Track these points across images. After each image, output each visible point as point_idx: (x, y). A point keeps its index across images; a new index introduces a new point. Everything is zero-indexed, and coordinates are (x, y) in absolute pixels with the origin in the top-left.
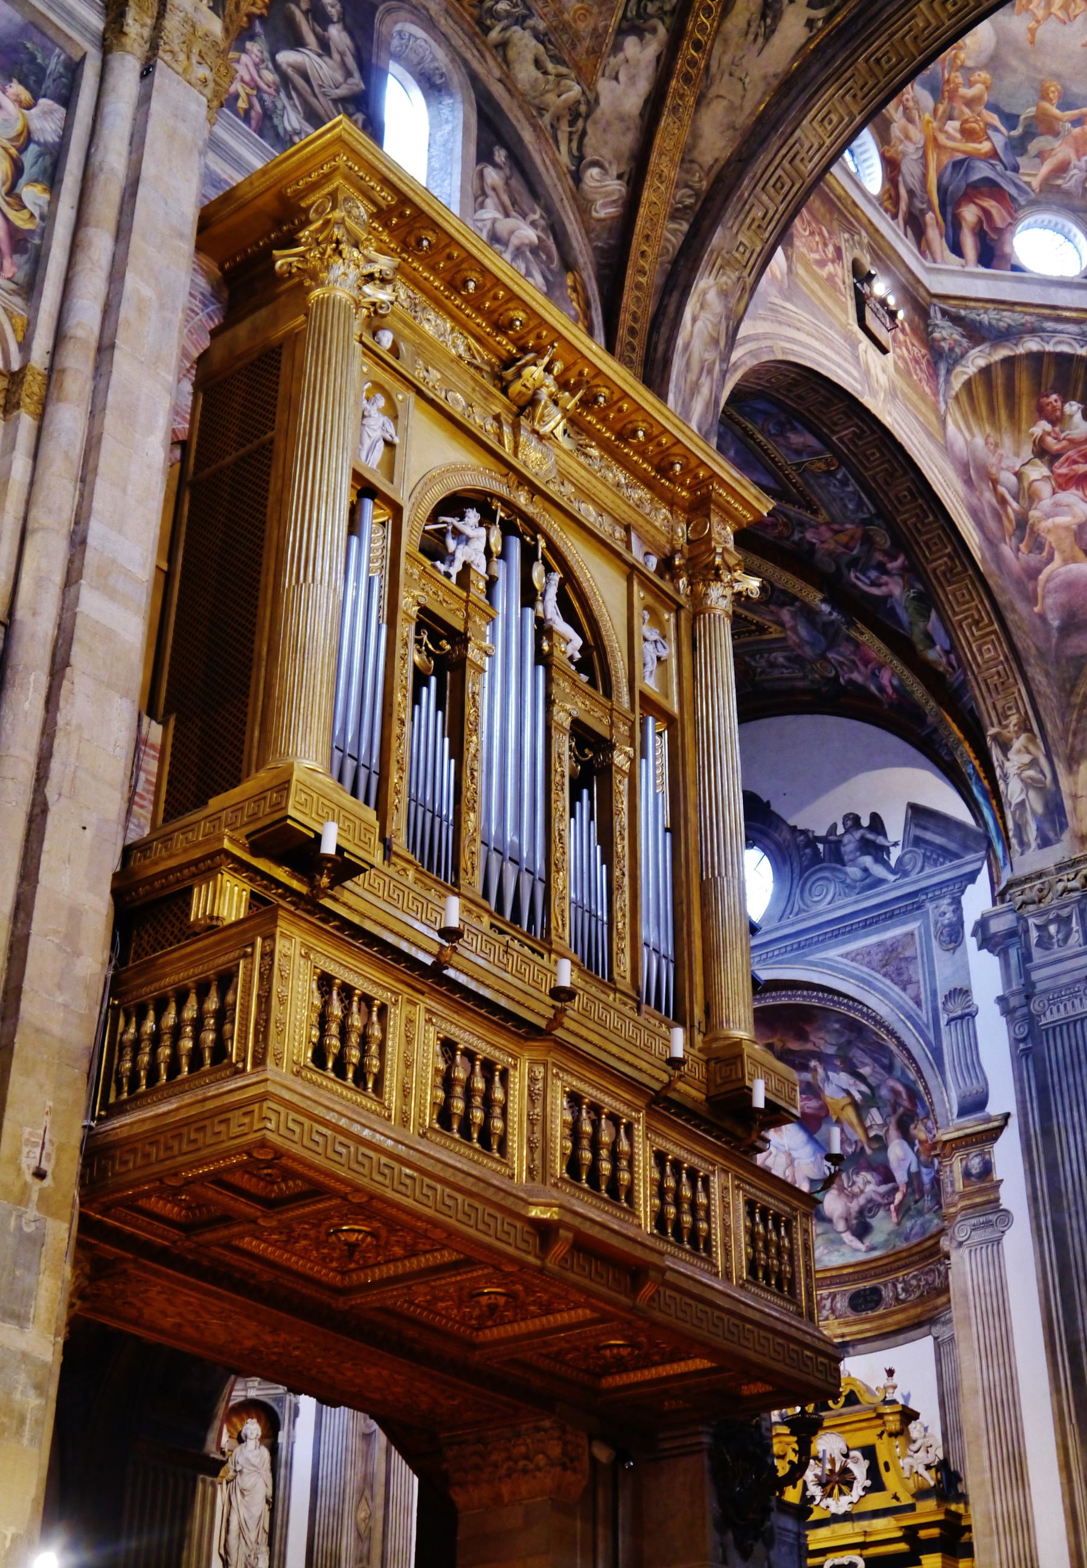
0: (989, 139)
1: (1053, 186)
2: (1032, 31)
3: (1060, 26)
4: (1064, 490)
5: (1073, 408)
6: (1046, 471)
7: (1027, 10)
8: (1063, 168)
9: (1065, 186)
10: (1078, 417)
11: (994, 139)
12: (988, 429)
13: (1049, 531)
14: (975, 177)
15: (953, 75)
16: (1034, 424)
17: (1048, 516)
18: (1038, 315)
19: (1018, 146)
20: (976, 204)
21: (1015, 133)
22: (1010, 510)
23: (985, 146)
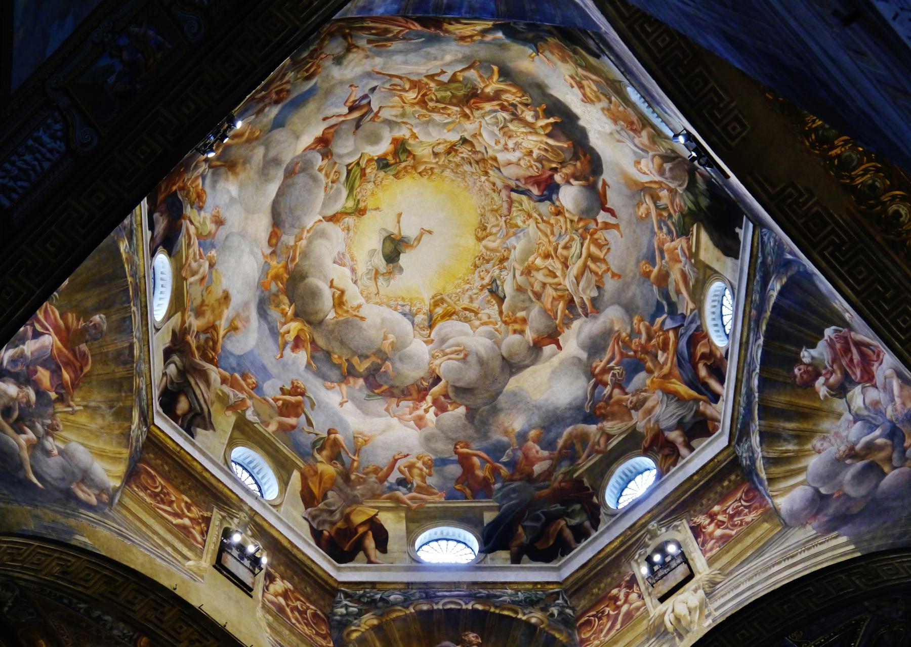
0: (668, 331)
2: (614, 275)
4: (873, 377)
5: (806, 355)
6: (858, 389)
7: (601, 277)
8: (684, 275)
10: (814, 352)
12: (809, 446)
13: (904, 404)
15: (633, 346)
16: (816, 393)
17: (892, 400)
20: (697, 363)
22: (880, 441)
23: (671, 334)
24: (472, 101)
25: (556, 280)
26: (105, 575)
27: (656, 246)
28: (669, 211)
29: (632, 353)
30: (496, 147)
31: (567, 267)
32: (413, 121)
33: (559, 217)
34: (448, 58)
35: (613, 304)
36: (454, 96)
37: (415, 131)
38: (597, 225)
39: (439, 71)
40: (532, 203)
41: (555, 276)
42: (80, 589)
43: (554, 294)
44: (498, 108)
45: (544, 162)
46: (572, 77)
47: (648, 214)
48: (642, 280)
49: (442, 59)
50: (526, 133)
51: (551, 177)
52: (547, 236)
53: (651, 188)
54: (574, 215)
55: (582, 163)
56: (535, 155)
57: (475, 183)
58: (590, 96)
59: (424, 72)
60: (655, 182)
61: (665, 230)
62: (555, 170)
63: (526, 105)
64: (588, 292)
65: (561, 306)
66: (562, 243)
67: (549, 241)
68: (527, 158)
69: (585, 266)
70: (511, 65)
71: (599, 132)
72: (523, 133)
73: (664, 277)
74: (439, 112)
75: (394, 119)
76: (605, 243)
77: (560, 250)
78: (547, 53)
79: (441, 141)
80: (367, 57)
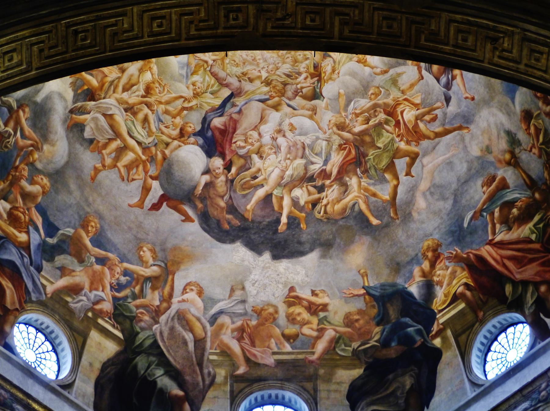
0: (28, 233)
1: (63, 299)
2: (97, 171)
3: (119, 180)
7: (100, 152)
8: (75, 290)
9: (72, 305)
11: (31, 235)
14: (6, 257)
15: (22, 166)
18: (12, 395)
19: (49, 252)
21: (49, 240)
23: (22, 237)
24: (353, 152)
25: (120, 88)
26: (447, 44)
27: (110, 255)
28: (140, 298)
29: (17, 163)
30: (287, 121)
31: (126, 110)
32: (379, 80)
33: (178, 131)
34: (421, 203)
35: (70, 154)
36: (373, 145)
37: (367, 69)
38: (153, 178)
39: (413, 173)
40: (207, 108)
41: (125, 90)
42: (458, 17)
43: (109, 79)
44: (328, 168)
45: (242, 161)
46: (324, 307)
47: (142, 261)
48: (81, 213)
49: (424, 194)
50: (283, 172)
51: (223, 155)
52: (168, 103)
53: (166, 282)
54: (172, 152)
55: (222, 209)
56: (255, 157)
57: (265, 61)
58: (297, 309)
59: (425, 160)
60: (171, 296)
61: (123, 279)
62: (228, 167)
63: (315, 204)
64: (92, 125)
65: (94, 82)
66: (152, 118)
67: (160, 103)
68: (257, 145)
69: (118, 135)
70: (367, 240)
71: (248, 271)
72: (287, 168)
73: (80, 255)
74: (368, 111)
75: (399, 70)
76: (130, 178)
77: (146, 110)
78: (360, 304)
79: (335, 76)
80: (488, 150)
